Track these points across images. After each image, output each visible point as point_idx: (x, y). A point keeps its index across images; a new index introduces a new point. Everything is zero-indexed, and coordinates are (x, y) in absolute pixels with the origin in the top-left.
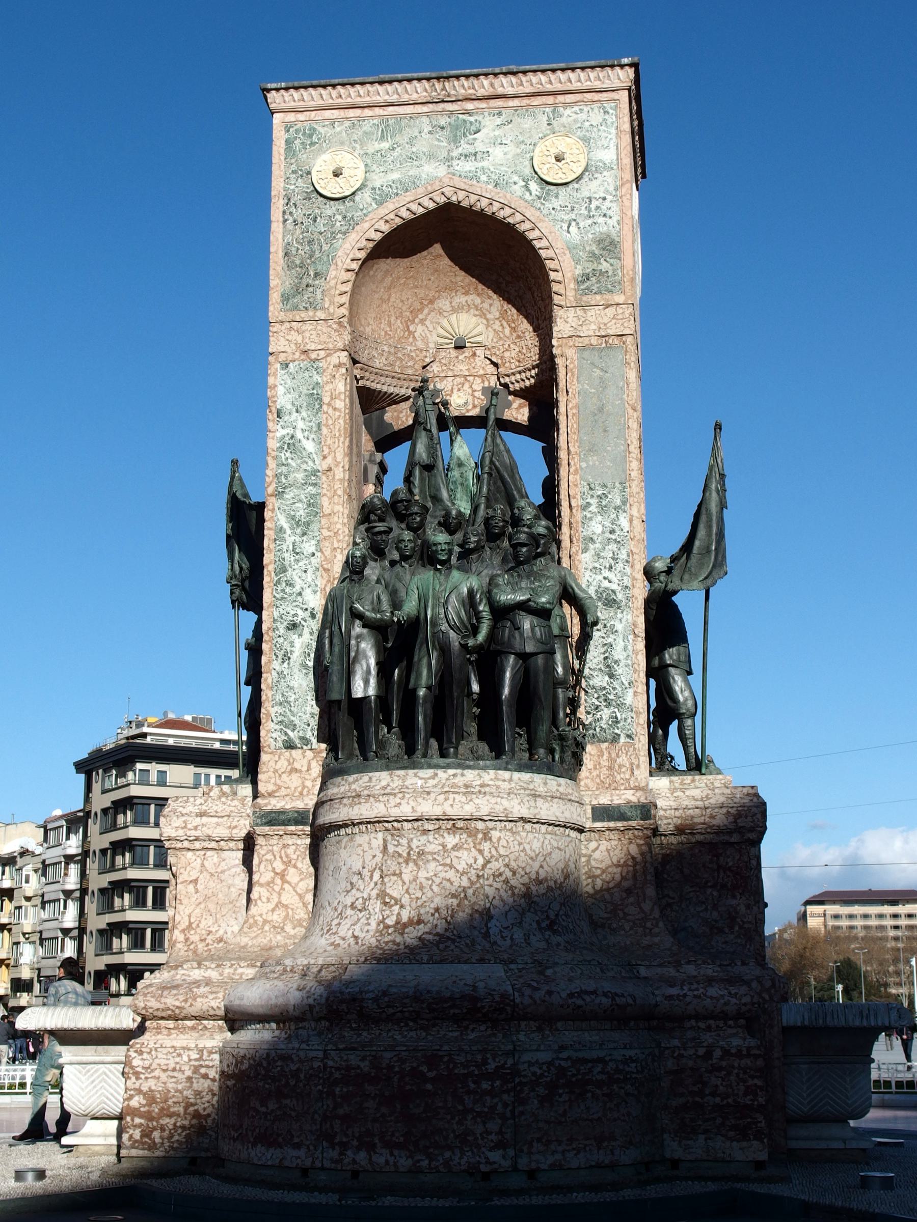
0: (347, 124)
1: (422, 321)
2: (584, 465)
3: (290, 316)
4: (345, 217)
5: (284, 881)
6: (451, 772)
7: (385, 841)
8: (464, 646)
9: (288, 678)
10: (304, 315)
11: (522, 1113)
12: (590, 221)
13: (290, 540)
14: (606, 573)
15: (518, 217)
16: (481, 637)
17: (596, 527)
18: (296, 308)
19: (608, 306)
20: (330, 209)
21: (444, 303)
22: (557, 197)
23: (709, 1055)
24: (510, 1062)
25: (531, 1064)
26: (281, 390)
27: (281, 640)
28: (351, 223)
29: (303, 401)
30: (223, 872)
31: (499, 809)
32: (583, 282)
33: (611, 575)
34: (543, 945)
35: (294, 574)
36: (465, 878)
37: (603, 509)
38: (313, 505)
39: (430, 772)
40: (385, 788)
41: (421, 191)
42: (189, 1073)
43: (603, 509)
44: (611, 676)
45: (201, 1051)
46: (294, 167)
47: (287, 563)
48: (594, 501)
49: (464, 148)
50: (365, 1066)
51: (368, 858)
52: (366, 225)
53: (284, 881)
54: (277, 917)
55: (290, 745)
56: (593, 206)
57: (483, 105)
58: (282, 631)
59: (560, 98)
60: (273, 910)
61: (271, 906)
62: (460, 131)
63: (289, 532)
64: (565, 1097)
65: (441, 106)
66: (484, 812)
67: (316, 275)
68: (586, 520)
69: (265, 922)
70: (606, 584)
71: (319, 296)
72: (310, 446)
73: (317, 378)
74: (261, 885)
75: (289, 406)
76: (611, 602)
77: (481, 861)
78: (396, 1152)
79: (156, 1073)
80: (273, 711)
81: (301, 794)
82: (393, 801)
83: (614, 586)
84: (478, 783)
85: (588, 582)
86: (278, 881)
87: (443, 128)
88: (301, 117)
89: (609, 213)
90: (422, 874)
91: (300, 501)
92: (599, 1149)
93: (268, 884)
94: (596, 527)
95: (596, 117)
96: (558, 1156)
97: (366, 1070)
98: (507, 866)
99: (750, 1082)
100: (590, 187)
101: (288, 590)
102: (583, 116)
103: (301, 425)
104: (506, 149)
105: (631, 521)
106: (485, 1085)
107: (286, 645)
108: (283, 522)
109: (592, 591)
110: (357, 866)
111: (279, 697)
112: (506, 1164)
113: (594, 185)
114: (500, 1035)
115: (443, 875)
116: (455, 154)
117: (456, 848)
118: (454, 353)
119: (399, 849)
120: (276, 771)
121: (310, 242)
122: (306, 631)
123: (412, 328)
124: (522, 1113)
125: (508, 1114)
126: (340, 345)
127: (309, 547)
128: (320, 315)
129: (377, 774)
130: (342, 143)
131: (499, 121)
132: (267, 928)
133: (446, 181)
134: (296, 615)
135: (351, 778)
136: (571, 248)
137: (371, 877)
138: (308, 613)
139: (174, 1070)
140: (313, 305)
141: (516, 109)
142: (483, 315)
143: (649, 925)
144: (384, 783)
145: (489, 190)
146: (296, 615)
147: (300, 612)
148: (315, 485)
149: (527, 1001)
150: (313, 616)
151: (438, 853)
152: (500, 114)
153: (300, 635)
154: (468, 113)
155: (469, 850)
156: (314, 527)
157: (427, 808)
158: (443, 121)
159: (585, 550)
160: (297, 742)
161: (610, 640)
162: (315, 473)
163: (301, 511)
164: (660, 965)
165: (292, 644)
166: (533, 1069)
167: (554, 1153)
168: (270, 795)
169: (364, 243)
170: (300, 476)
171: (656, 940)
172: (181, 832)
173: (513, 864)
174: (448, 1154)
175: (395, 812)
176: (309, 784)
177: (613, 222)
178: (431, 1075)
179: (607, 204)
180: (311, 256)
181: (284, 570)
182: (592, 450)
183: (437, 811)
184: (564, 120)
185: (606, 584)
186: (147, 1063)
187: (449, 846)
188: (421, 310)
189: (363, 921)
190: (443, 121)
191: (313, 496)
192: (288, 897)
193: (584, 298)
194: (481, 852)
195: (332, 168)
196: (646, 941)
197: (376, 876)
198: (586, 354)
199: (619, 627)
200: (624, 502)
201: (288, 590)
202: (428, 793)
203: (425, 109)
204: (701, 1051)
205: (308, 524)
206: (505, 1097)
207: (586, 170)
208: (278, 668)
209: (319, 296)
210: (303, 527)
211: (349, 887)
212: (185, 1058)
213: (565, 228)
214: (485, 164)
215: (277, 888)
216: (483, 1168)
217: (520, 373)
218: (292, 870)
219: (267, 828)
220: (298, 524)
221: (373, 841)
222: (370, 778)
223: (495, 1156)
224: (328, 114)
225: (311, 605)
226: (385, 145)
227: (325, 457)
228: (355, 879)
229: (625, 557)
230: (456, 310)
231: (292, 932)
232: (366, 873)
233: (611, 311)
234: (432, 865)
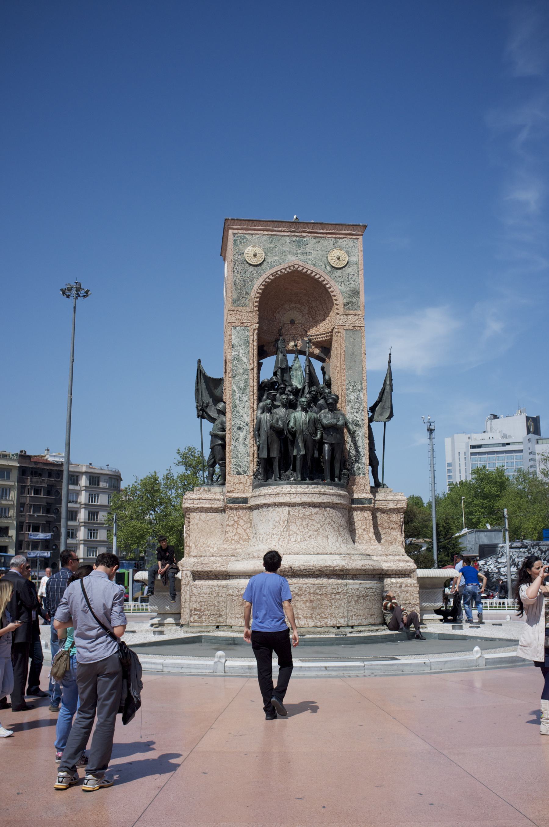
0: (258, 236)
1: (278, 312)
2: (347, 374)
3: (236, 309)
4: (257, 272)
5: (238, 524)
6: (313, 486)
7: (289, 511)
8: (314, 441)
9: (238, 448)
10: (242, 309)
11: (350, 606)
12: (349, 283)
13: (238, 395)
14: (356, 414)
15: (322, 279)
16: (319, 436)
17: (352, 397)
18: (239, 306)
19: (355, 315)
20: (251, 268)
21: (287, 306)
22: (337, 272)
23: (401, 587)
24: (346, 588)
25: (352, 589)
27: (235, 433)
28: (260, 275)
29: (242, 342)
30: (208, 520)
31: (330, 501)
32: (346, 305)
33: (357, 415)
34: (346, 548)
35: (239, 408)
36: (319, 525)
37: (354, 390)
39: (306, 486)
40: (289, 491)
41: (286, 265)
42: (215, 595)
43: (354, 390)
45: (219, 587)
46: (237, 251)
47: (237, 404)
48: (351, 387)
49: (302, 250)
50: (296, 590)
51: (282, 515)
52: (266, 276)
53: (238, 524)
54: (236, 538)
55: (239, 473)
56: (350, 277)
57: (310, 235)
58: (235, 430)
59: (337, 236)
60: (235, 535)
61: (234, 534)
62: (300, 243)
63: (237, 392)
64: (362, 601)
65: (293, 234)
66: (325, 501)
67: (246, 293)
68: (348, 394)
69: (232, 539)
70: (355, 418)
71: (247, 302)
72: (245, 360)
73: (247, 333)
74: (230, 526)
75: (237, 344)
76: (357, 425)
77: (324, 519)
78: (308, 620)
79: (203, 595)
80: (232, 460)
81: (244, 492)
82: (293, 496)
83: (358, 419)
84: (323, 490)
85: (350, 417)
86: (236, 524)
87: (294, 242)
88: (240, 232)
89: (356, 280)
90: (304, 523)
91: (242, 380)
93: (232, 525)
94: (352, 397)
95: (351, 243)
96: (360, 621)
97: (296, 592)
99: (415, 595)
100: (348, 270)
101: (237, 414)
102: (346, 243)
103: (241, 351)
104: (318, 252)
105: (364, 396)
106: (338, 597)
107: (237, 436)
109: (350, 420)
110: (277, 519)
111: (234, 455)
112: (345, 624)
113: (350, 269)
115: (311, 523)
116: (299, 252)
117: (316, 513)
118: (290, 326)
119: (295, 514)
120: (234, 483)
121: (244, 281)
122: (245, 430)
123: (275, 315)
124: (350, 606)
125: (345, 607)
126: (256, 321)
127: (245, 398)
128: (248, 309)
129: (285, 486)
130: (256, 243)
131: (315, 241)
132: (233, 542)
133: (296, 262)
134: (240, 424)
135: (273, 487)
136: (342, 292)
137: (284, 523)
138: (245, 424)
139: (209, 594)
141: (321, 237)
142: (301, 312)
143: (372, 541)
144: (288, 490)
145: (312, 268)
146: (240, 424)
147: (242, 423)
148: (247, 375)
149: (350, 568)
150: (247, 425)
151: (309, 515)
152: (315, 239)
153: (242, 432)
154: (304, 237)
155: (320, 514)
156: (247, 391)
157: (306, 499)
158: (294, 239)
159: (348, 405)
160: (242, 472)
162: (247, 370)
163: (242, 385)
164: (380, 556)
165: (239, 435)
166: (353, 591)
167: (359, 619)
168: (231, 492)
169: (264, 283)
170: (241, 371)
172: (192, 505)
173: (334, 519)
174: (326, 620)
175: (294, 500)
176: (247, 488)
177: (357, 284)
178: (320, 593)
179: (355, 277)
180: (244, 286)
181: (236, 407)
182: (350, 368)
183: (310, 500)
184: (339, 243)
185: (355, 418)
186: (199, 592)
187: (313, 513)
189: (282, 539)
190: (294, 239)
191: (246, 379)
192: (240, 531)
193: (347, 311)
195: (252, 253)
196: (372, 547)
197: (286, 522)
198: (348, 332)
199: (360, 434)
200: (362, 388)
201: (237, 414)
202: (306, 493)
203: (288, 234)
204: (398, 585)
205: (245, 389)
206: (344, 600)
207: (348, 263)
208: (234, 444)
209: (247, 302)
210: (243, 391)
211: (274, 527)
212: (214, 590)
213: (340, 284)
214: (310, 257)
215: (236, 527)
216: (338, 625)
217: (316, 335)
218: (241, 521)
219: (231, 505)
220: (241, 389)
221: (284, 511)
222: (282, 488)
223: (342, 621)
224: (250, 232)
225: (246, 420)
226: (272, 246)
227: (251, 364)
228: (277, 524)
229: (362, 408)
230: (292, 309)
231: (243, 544)
232: (281, 522)
233: (356, 317)
234: (307, 520)
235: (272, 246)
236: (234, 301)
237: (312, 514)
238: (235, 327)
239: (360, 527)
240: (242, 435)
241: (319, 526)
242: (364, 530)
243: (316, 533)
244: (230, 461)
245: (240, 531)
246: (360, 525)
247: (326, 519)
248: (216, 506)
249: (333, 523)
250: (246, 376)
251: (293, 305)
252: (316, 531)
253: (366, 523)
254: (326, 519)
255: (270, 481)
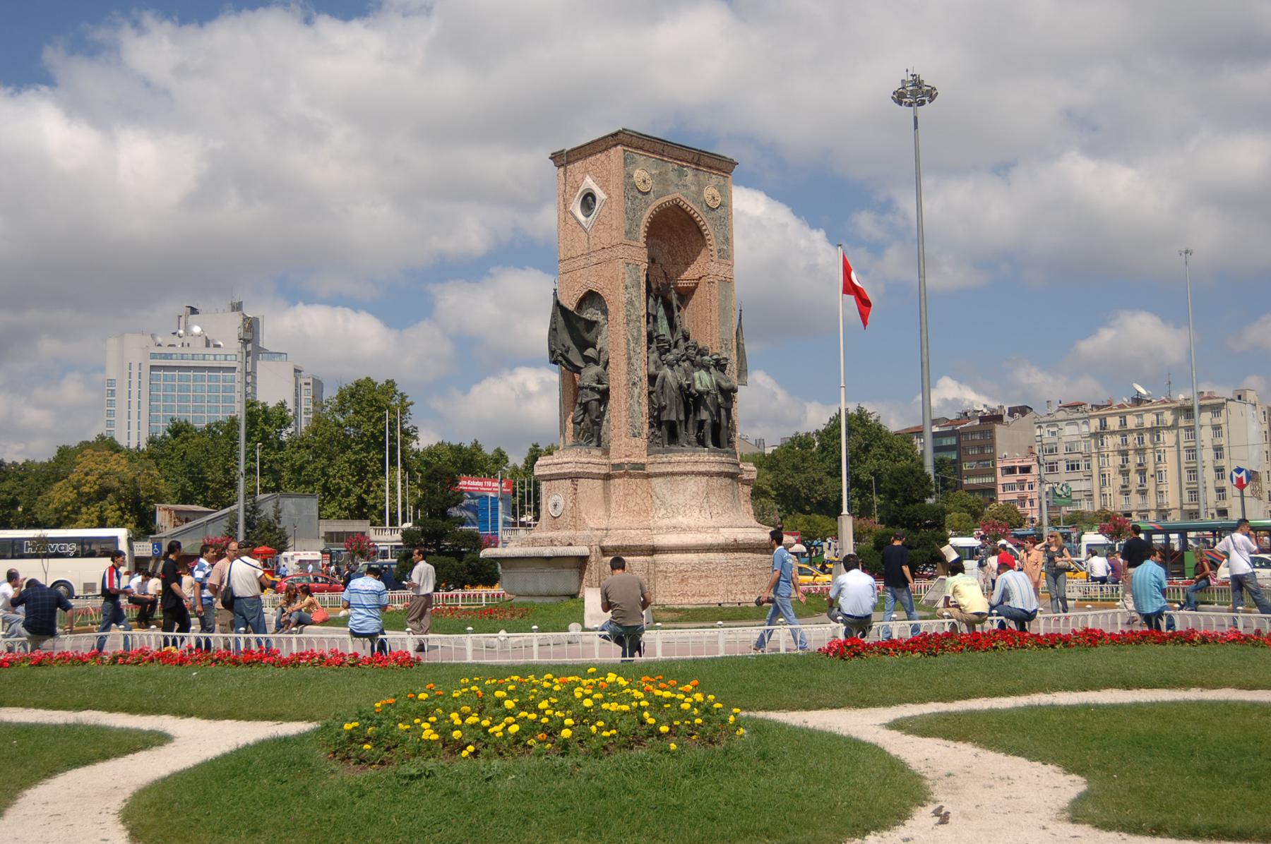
3: (626, 241)
28: (648, 205)
35: (633, 361)
38: (639, 330)
72: (637, 304)
140: (637, 240)
192: (639, 501)
236: (627, 233)
238: (628, 264)
240: (637, 391)
245: (639, 501)
248: (603, 472)
255: (674, 447)
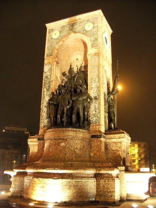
1: (71, 57)
19: (96, 49)
20: (54, 40)
21: (75, 53)
26: (46, 69)
44: (96, 112)
48: (93, 81)
83: (96, 96)
92: (80, 198)
98: (70, 145)
108: (45, 90)
114: (61, 176)
123: (70, 58)
161: (96, 105)
164: (99, 164)
170: (48, 82)
171: (101, 159)
179: (96, 32)
187: (60, 142)
188: (71, 55)
194: (65, 143)
226: (63, 29)
235: (63, 29)
237: (59, 142)
239: (96, 150)
241: (62, 148)
242: (98, 151)
243: (60, 152)
244: (41, 122)
246: (96, 148)
247: (66, 145)
249: (70, 147)
250: (49, 84)
251: (77, 52)
252: (60, 151)
253: (99, 147)
254: (66, 145)
